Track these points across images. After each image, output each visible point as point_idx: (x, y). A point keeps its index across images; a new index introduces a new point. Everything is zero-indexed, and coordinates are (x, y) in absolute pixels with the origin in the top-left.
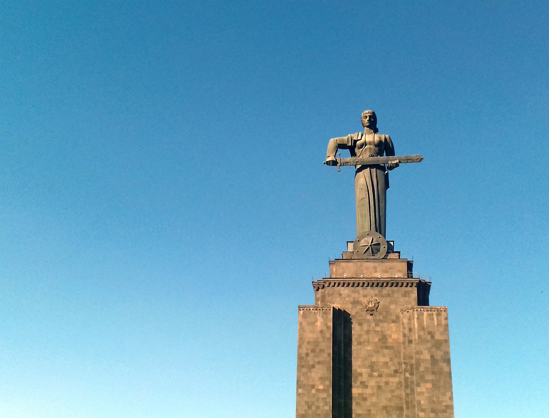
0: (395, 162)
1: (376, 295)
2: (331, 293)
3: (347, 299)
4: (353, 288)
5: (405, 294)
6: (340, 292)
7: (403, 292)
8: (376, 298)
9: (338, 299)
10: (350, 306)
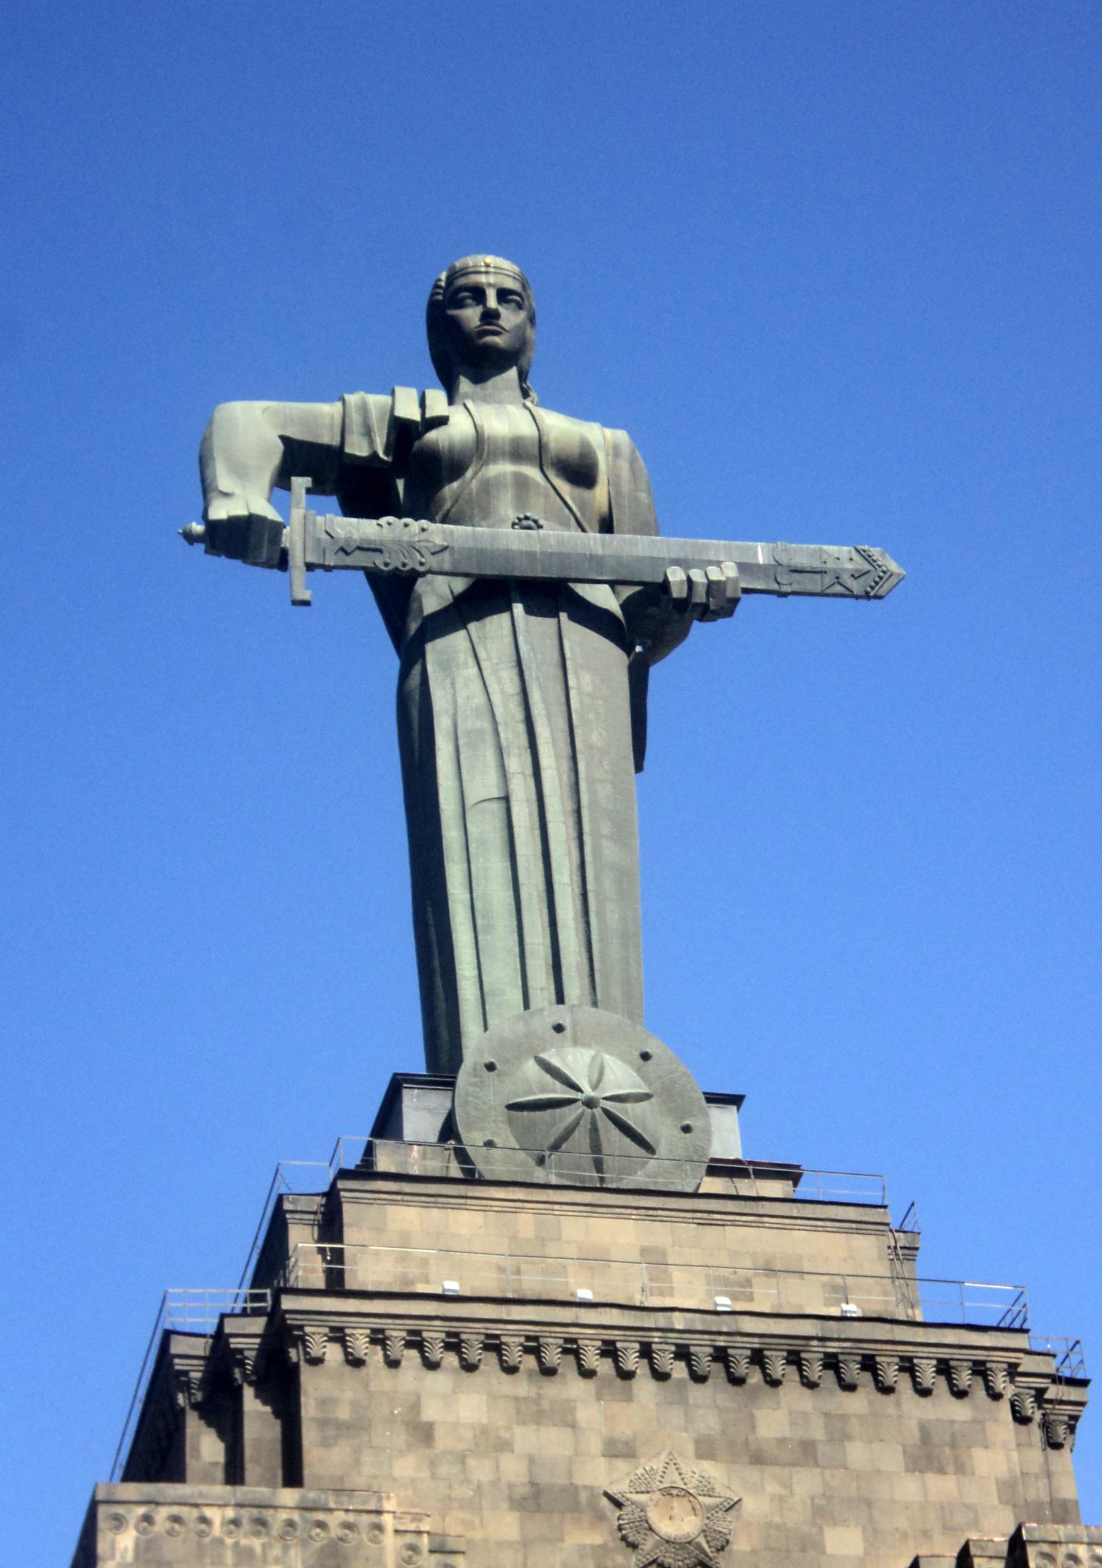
0: (715, 574)
1: (705, 1450)
2: (343, 1413)
3: (481, 1470)
4: (521, 1386)
5: (928, 1454)
6: (416, 1407)
7: (913, 1435)
8: (712, 1470)
9: (406, 1467)
10: (506, 1525)
